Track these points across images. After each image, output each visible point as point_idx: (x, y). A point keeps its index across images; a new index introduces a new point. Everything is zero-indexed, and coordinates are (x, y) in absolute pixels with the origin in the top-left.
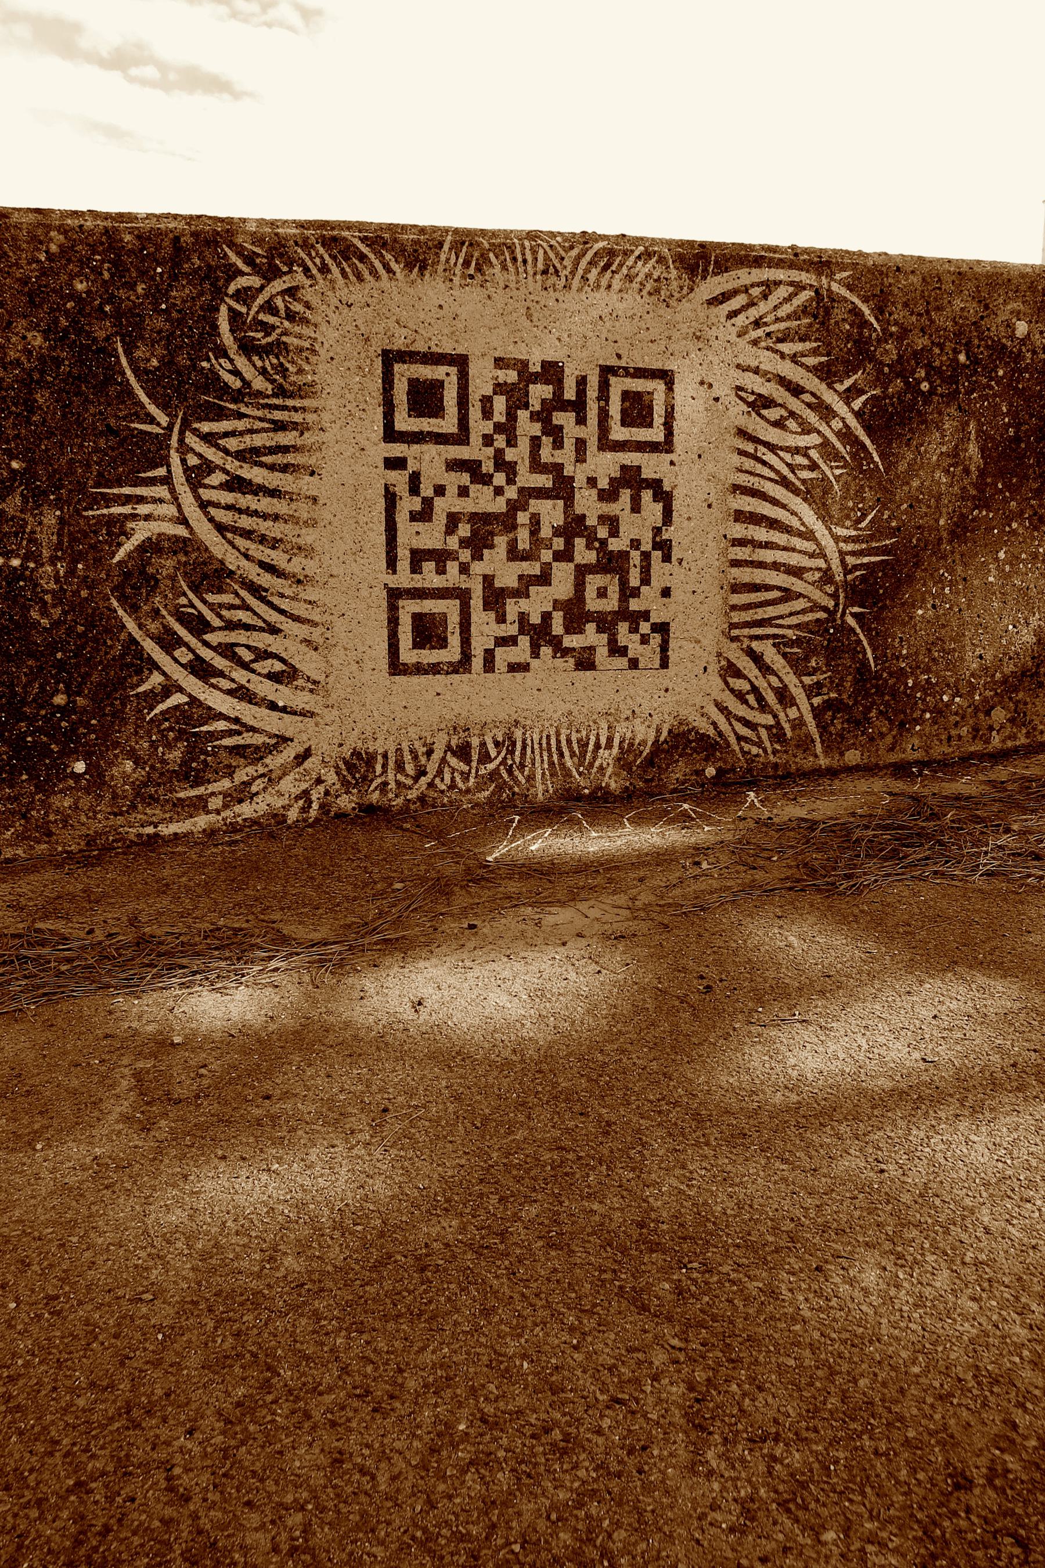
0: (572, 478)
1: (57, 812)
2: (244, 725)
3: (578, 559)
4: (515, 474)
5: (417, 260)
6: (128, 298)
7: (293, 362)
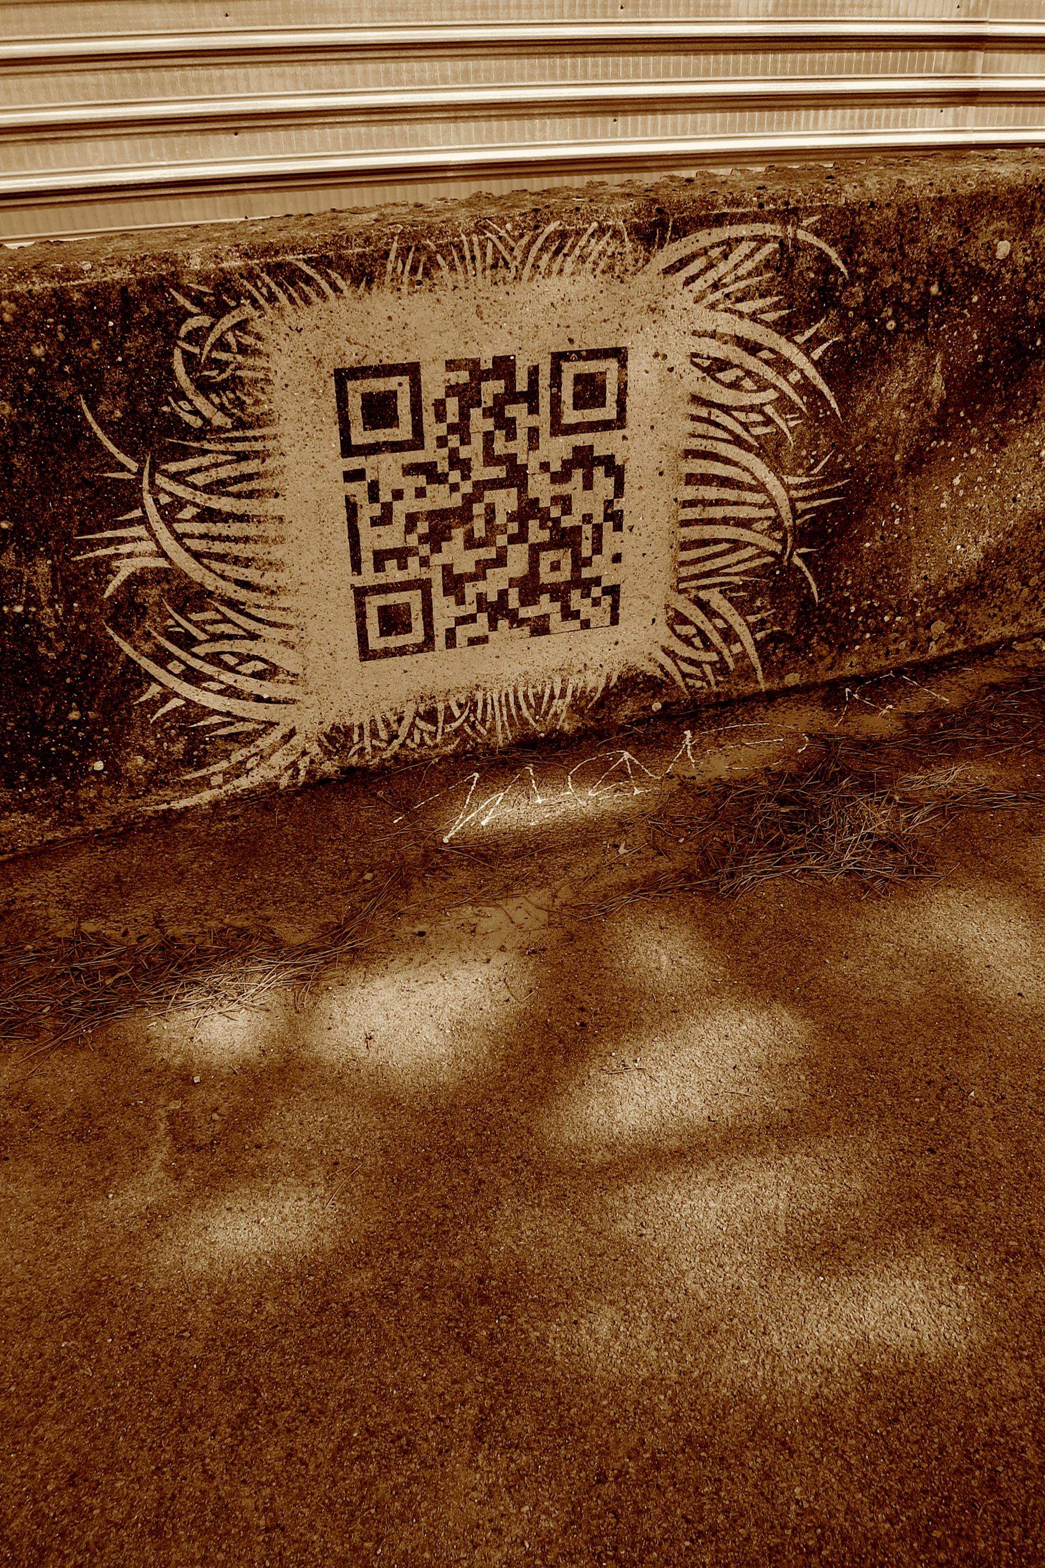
0: (525, 466)
1: (84, 802)
2: (235, 717)
3: (532, 539)
4: (470, 470)
5: (363, 274)
6: (85, 356)
7: (249, 394)
